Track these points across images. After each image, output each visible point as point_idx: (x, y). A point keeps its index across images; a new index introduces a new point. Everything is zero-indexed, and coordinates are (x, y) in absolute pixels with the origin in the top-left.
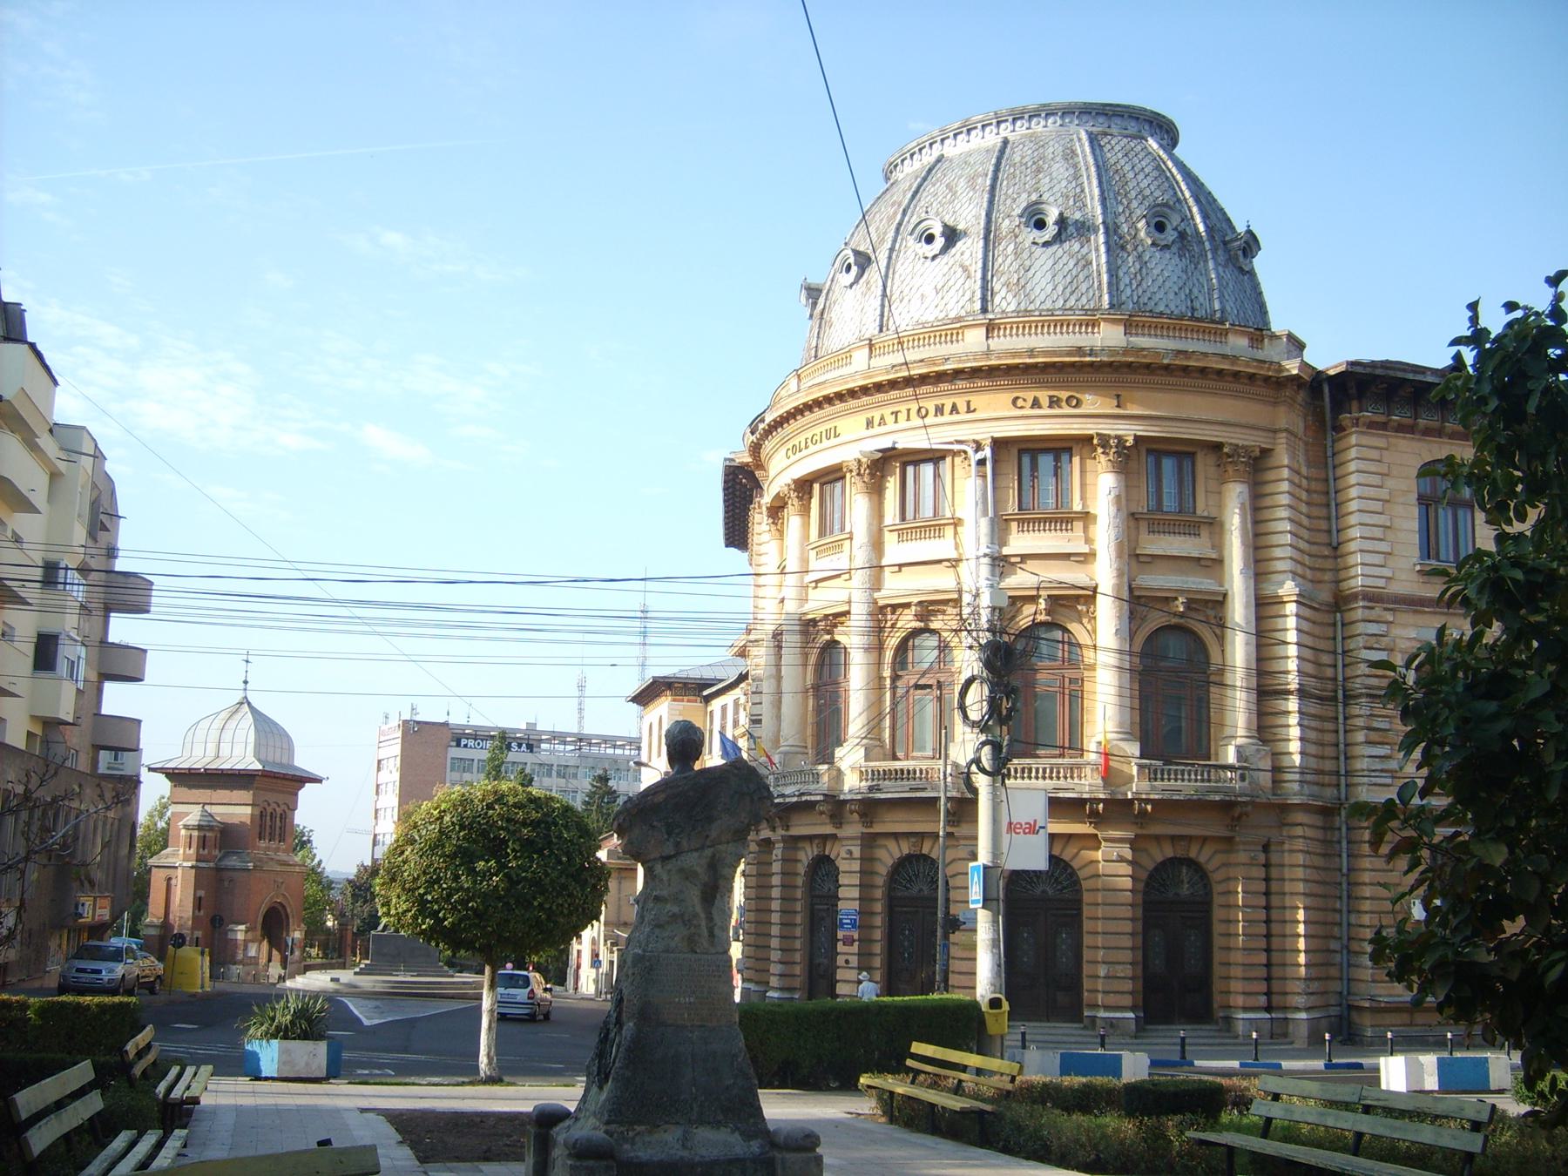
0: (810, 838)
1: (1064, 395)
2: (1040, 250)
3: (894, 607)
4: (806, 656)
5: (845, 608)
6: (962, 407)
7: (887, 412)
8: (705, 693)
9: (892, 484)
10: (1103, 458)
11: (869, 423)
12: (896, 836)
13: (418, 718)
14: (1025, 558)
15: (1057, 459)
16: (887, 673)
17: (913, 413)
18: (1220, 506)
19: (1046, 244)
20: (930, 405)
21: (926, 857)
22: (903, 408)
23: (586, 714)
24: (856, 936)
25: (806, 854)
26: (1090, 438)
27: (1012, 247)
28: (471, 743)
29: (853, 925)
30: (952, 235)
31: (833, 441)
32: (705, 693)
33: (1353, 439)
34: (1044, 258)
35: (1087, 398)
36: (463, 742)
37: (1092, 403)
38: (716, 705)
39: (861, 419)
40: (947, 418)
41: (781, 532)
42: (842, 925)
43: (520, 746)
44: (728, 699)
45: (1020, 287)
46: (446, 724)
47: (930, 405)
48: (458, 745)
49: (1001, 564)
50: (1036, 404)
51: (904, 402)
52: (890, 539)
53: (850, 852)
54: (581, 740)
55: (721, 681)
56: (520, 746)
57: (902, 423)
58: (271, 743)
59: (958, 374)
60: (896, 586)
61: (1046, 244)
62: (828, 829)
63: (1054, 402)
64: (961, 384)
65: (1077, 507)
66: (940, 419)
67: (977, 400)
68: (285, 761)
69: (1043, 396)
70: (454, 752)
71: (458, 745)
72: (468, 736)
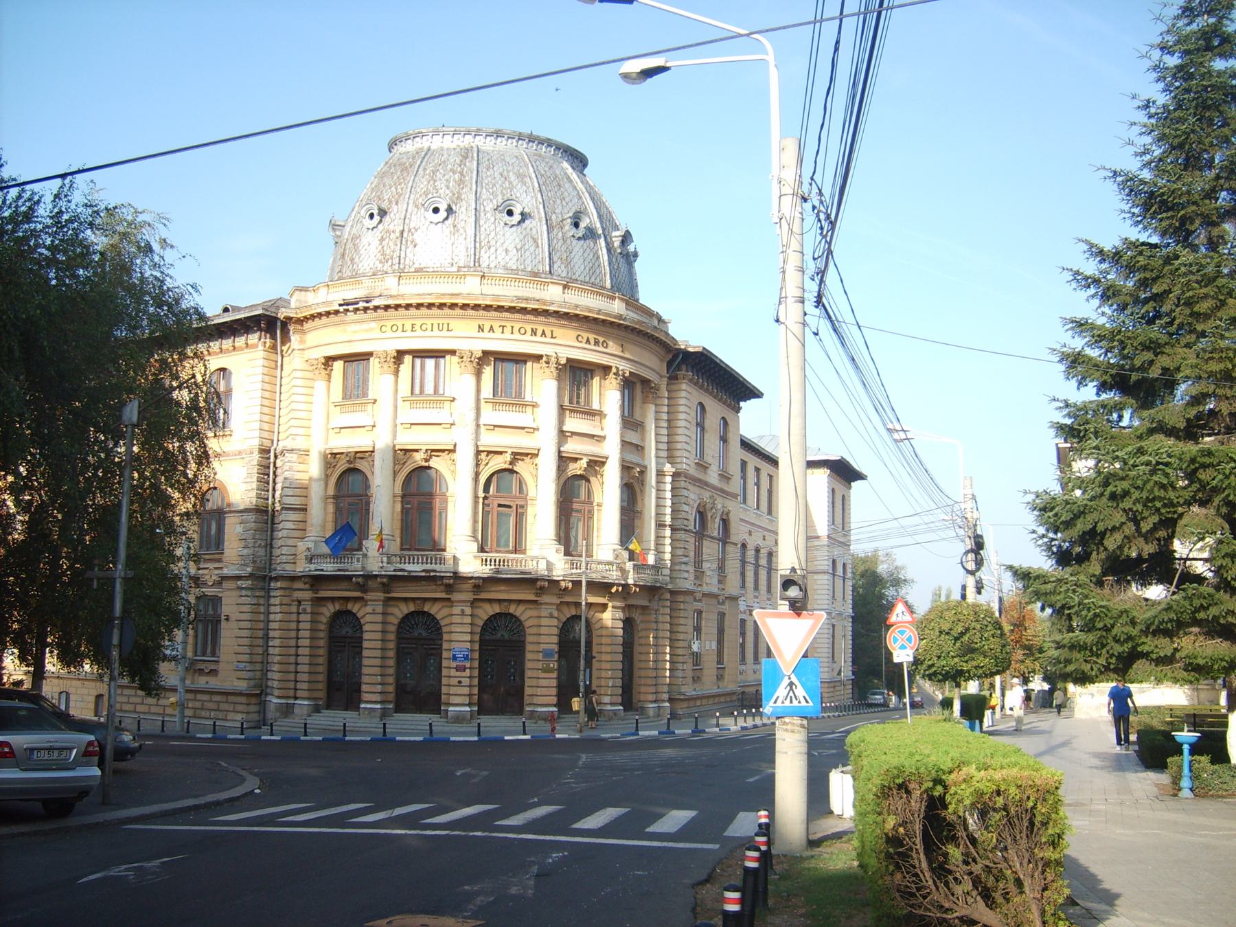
1: (601, 339)
2: (575, 242)
3: (489, 452)
4: (395, 474)
5: (451, 447)
6: (548, 333)
7: (496, 325)
9: (488, 372)
10: (614, 382)
11: (481, 328)
14: (573, 434)
15: (586, 376)
16: (481, 494)
17: (516, 329)
18: (644, 415)
19: (579, 239)
20: (528, 327)
21: (512, 616)
22: (509, 325)
24: (468, 665)
26: (609, 368)
27: (560, 235)
29: (466, 658)
30: (524, 216)
31: (445, 333)
33: (684, 386)
34: (578, 246)
35: (610, 343)
37: (613, 348)
39: (475, 324)
40: (538, 338)
41: (329, 375)
42: (454, 658)
45: (568, 262)
47: (528, 327)
49: (563, 435)
50: (588, 341)
51: (529, 323)
52: (486, 409)
53: (463, 611)
57: (507, 335)
59: (556, 314)
60: (489, 440)
61: (579, 239)
63: (597, 343)
64: (552, 320)
65: (595, 406)
66: (534, 338)
67: (558, 332)
69: (592, 337)
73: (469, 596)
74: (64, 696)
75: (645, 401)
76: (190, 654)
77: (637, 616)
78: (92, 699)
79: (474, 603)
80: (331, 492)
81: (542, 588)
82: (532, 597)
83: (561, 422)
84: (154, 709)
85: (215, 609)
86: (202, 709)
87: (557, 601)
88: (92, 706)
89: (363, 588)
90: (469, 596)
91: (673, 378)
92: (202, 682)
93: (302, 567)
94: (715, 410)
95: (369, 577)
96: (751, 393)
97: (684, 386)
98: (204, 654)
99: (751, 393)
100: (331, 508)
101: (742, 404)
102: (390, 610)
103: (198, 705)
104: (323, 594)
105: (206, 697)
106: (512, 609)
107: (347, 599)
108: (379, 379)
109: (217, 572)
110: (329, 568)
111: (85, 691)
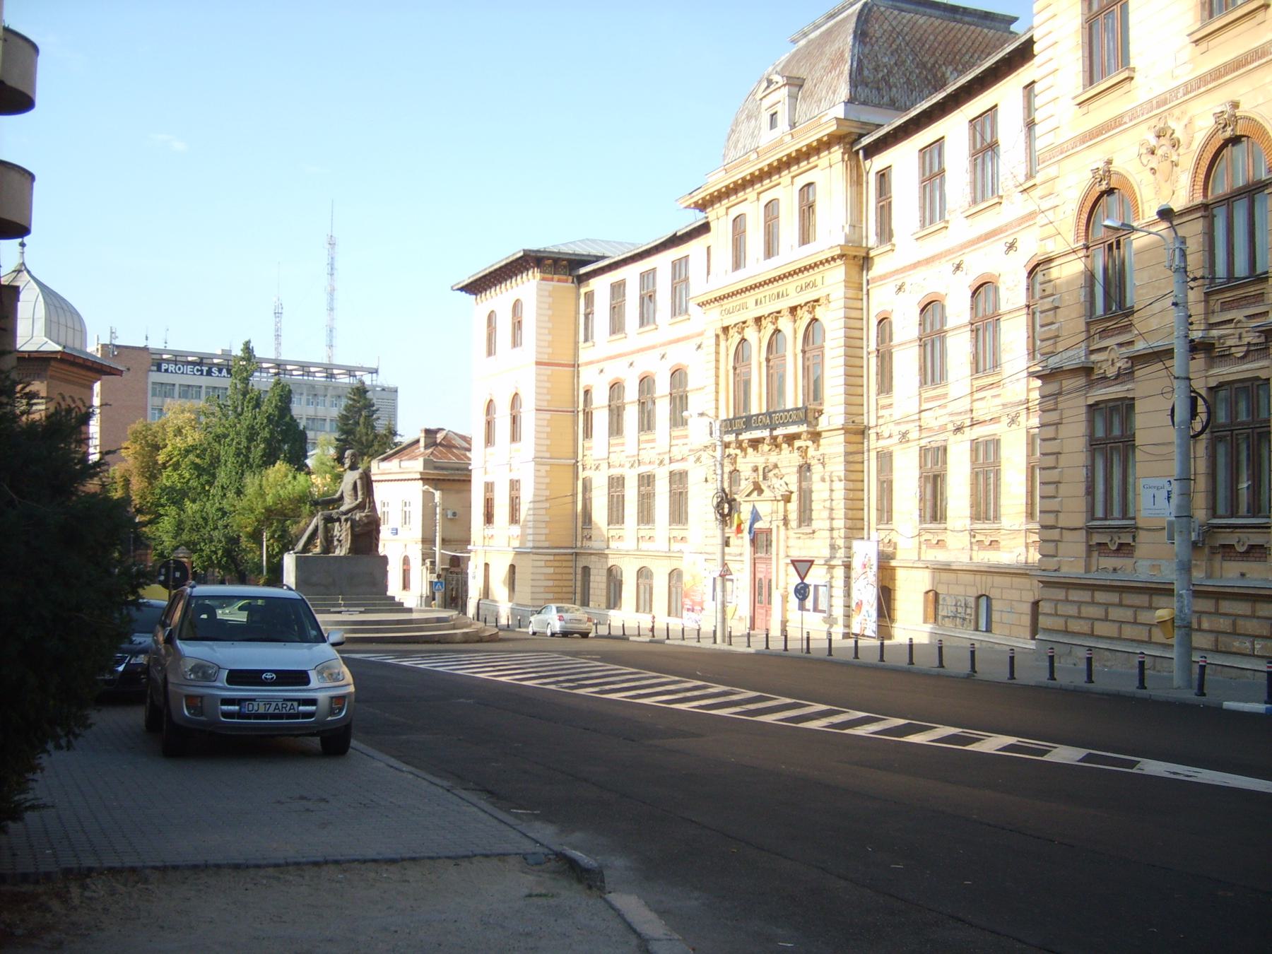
8: (583, 271)
13: (117, 342)
23: (283, 340)
28: (172, 367)
32: (583, 271)
36: (164, 366)
38: (600, 286)
43: (220, 371)
44: (630, 273)
46: (145, 349)
48: (159, 370)
54: (278, 366)
55: (603, 258)
56: (220, 371)
58: (62, 320)
68: (77, 346)
70: (155, 377)
71: (159, 370)
72: (167, 361)
74: (983, 601)
76: (1201, 514)
78: (1027, 608)
84: (1128, 631)
85: (1253, 409)
86: (1234, 633)
88: (1026, 620)
92: (1231, 573)
98: (1233, 514)
103: (1224, 624)
105: (1242, 608)
109: (1254, 323)
111: (1015, 595)
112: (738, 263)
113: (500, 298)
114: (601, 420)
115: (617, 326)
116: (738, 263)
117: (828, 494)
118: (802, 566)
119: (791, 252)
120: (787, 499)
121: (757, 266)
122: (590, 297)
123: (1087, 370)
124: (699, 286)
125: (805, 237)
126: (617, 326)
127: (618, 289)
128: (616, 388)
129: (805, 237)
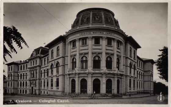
0: (72, 77)
12: (94, 77)
25: (71, 79)
33: (128, 44)
62: (74, 76)
73: (91, 76)
75: (121, 45)
77: (120, 79)
79: (92, 77)
80: (71, 62)
81: (102, 74)
82: (101, 76)
83: (106, 48)
87: (105, 76)
89: (75, 75)
90: (91, 76)
91: (126, 43)
93: (68, 73)
94: (133, 49)
95: (76, 74)
96: (139, 47)
97: (128, 44)
99: (139, 47)
100: (71, 64)
101: (138, 49)
102: (79, 78)
104: (70, 77)
106: (98, 78)
107: (73, 77)
108: (77, 44)
110: (71, 73)
112: (31, 66)
113: (10, 67)
114: (20, 77)
115: (21, 69)
116: (31, 66)
117: (37, 84)
118: (35, 90)
119: (35, 65)
120: (34, 84)
121: (32, 66)
122: (19, 66)
123: (56, 76)
124: (28, 67)
125: (36, 64)
126: (21, 69)
127: (21, 66)
128: (21, 74)
129: (36, 64)
